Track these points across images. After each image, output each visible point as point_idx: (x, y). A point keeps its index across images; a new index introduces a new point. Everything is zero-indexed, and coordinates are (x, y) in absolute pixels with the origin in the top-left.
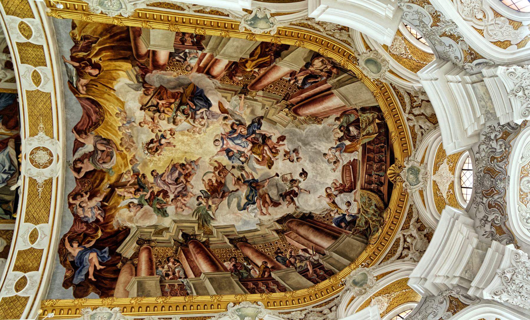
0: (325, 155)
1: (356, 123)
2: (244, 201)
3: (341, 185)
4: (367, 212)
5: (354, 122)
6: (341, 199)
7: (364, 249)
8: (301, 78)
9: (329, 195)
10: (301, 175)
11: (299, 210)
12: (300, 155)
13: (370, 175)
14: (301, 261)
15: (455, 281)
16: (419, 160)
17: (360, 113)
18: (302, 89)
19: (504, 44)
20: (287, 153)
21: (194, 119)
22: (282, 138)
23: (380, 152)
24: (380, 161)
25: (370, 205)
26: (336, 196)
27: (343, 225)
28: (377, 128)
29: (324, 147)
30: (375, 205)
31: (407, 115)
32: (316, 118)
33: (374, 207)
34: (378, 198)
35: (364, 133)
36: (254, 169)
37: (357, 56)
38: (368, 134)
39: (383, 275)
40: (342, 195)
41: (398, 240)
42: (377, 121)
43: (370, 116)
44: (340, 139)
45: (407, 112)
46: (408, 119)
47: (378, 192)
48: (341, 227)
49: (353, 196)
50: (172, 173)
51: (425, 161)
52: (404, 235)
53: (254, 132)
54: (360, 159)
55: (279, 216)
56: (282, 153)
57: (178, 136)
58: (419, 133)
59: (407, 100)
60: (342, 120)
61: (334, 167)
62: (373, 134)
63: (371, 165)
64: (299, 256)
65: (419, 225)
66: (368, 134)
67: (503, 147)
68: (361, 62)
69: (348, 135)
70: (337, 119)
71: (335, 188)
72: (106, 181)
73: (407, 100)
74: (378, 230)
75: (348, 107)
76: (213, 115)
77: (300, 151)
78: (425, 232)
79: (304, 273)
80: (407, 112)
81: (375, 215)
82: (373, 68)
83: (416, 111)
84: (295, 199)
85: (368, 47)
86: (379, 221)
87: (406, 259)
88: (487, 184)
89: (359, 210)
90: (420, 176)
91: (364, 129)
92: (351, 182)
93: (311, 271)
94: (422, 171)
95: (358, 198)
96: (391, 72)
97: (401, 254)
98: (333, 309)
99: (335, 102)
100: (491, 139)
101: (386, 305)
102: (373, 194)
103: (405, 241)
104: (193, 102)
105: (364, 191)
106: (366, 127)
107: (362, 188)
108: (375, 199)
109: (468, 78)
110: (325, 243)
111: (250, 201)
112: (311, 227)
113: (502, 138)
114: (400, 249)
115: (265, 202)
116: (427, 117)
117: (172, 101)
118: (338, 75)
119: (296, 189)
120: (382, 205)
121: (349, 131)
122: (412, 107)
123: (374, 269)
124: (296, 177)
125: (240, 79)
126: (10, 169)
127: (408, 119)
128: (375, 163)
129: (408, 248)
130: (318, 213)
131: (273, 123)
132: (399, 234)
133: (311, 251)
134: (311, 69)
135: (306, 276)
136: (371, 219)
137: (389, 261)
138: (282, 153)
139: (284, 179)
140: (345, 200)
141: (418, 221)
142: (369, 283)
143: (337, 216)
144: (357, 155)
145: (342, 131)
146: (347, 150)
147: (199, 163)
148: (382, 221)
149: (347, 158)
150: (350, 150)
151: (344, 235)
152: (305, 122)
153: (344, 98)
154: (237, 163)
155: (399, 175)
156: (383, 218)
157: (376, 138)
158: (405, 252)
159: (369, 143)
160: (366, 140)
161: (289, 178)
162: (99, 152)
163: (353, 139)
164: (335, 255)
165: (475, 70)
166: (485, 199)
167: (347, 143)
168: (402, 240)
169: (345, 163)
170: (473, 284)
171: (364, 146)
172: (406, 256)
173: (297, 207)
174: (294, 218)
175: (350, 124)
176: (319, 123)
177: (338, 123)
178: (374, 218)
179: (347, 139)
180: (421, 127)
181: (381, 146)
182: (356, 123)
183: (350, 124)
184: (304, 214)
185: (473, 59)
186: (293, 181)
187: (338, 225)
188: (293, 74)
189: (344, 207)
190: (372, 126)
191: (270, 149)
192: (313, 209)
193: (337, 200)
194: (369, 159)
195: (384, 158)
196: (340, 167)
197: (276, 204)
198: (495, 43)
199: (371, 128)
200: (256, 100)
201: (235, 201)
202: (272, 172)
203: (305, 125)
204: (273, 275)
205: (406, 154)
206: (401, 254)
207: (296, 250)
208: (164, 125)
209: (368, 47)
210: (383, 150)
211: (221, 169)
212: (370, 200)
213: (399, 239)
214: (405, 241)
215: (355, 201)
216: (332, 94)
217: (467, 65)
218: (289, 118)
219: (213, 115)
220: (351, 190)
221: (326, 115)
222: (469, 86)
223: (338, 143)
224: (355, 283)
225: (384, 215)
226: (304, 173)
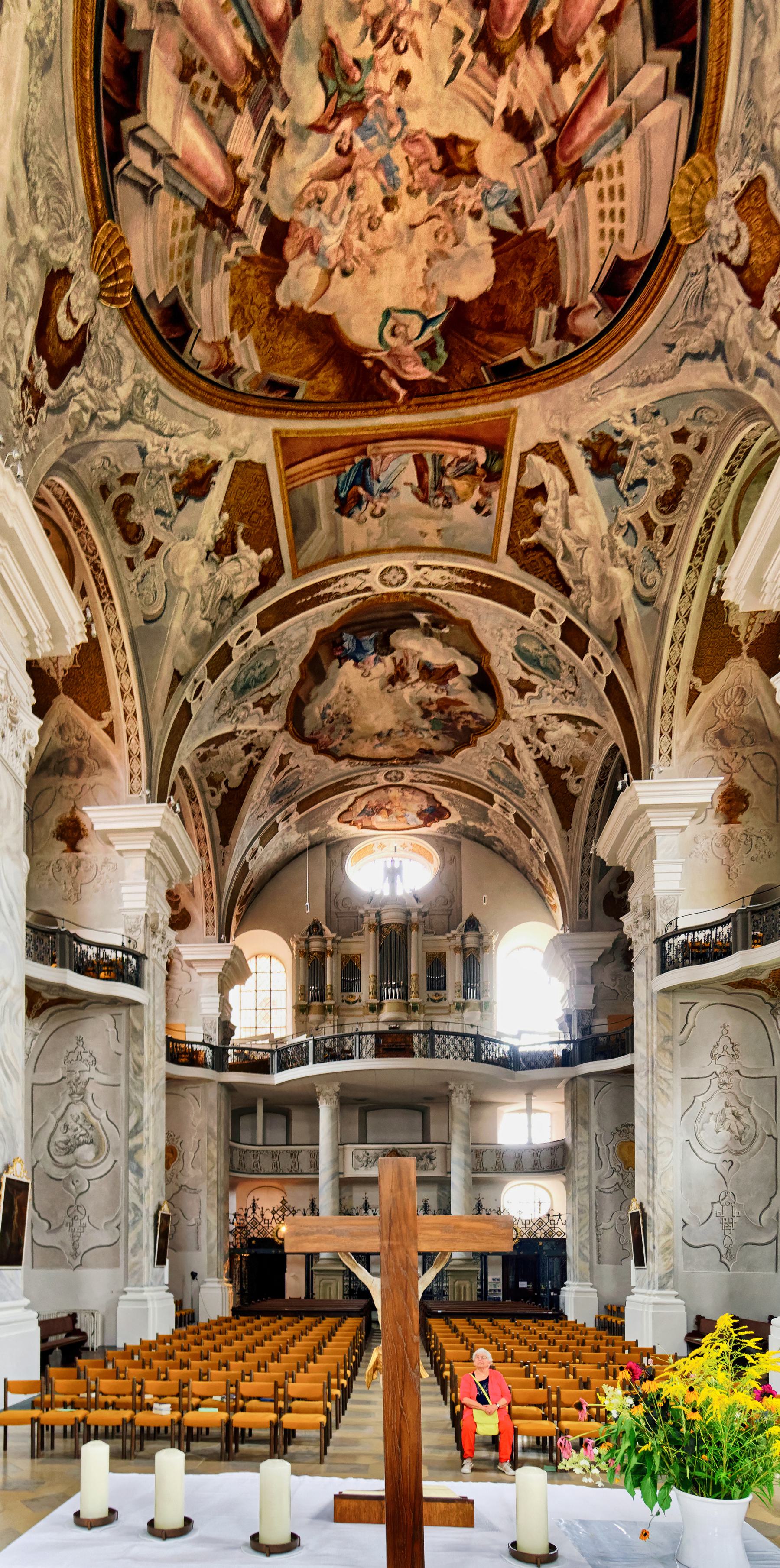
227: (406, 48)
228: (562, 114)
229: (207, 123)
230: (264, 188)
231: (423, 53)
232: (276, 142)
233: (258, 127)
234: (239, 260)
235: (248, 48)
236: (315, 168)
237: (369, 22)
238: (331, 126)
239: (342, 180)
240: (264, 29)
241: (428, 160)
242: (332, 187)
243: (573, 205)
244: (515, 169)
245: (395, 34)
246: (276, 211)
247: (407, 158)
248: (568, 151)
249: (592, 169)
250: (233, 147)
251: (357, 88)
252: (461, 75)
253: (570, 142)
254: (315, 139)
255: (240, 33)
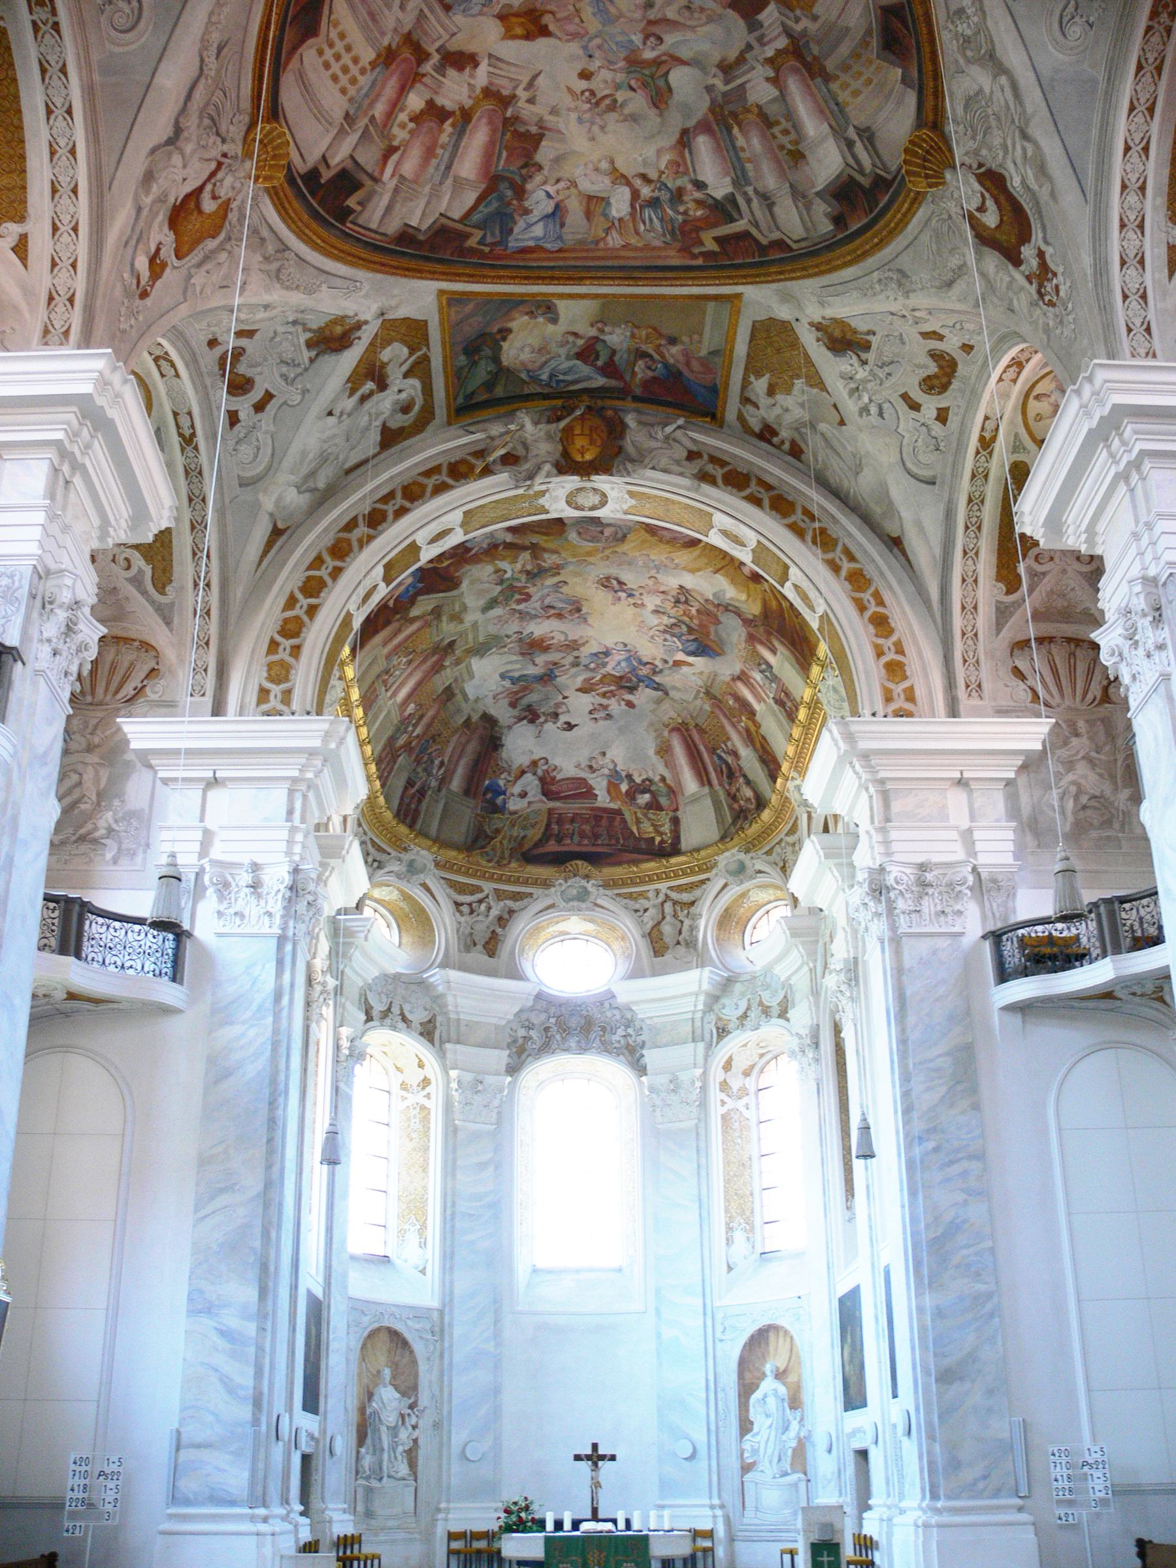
0: (604, 754)
1: (654, 805)
2: (516, 674)
3: (554, 778)
4: (514, 825)
5: (657, 802)
6: (530, 782)
7: (457, 848)
8: (730, 759)
9: (534, 763)
10: (568, 723)
11: (505, 731)
12: (601, 722)
13: (572, 821)
14: (425, 770)
15: (453, 1016)
16: (599, 901)
17: (671, 814)
18: (713, 751)
19: (728, 1066)
20: (605, 707)
21: (665, 632)
22: (630, 705)
23: (610, 837)
24: (596, 836)
25: (524, 828)
26: (535, 774)
27: (489, 796)
28: (647, 836)
29: (619, 755)
30: (525, 837)
31: (664, 891)
32: (664, 751)
33: (522, 834)
34: (539, 836)
35: (639, 815)
36: (575, 676)
37: (751, 854)
38: (638, 822)
39: (428, 889)
40: (537, 782)
41: (479, 889)
42: (658, 839)
43: (667, 828)
44: (629, 777)
45: (669, 892)
46: (658, 892)
47: (547, 835)
48: (484, 795)
49: (537, 799)
50: (560, 600)
51: (597, 909)
52: (487, 897)
53: (640, 681)
54: (597, 805)
55: (493, 712)
56: (605, 702)
57: (631, 611)
58: (637, 906)
59: (686, 897)
60: (661, 785)
61: (583, 766)
62: (638, 829)
63: (587, 821)
64: (432, 762)
65: (506, 916)
66: (638, 822)
67: (616, 1045)
68: (742, 856)
69: (636, 790)
70: (663, 779)
71: (547, 771)
72: (545, 538)
73: (686, 897)
74: (489, 861)
75: (680, 799)
76: (671, 651)
77: (608, 722)
78: (499, 930)
79: (410, 783)
80: (669, 892)
81: (510, 841)
82: (734, 867)
83: (668, 907)
84: (525, 722)
85: (760, 872)
86: (502, 858)
87: (457, 914)
88: (573, 1022)
89: (515, 813)
90: (575, 903)
91: (645, 815)
92: (557, 793)
93: (413, 791)
94: (583, 905)
95: (534, 807)
96: (725, 885)
97: (462, 904)
98: (376, 864)
99: (690, 784)
100: (627, 1027)
101: (387, 898)
102: (542, 830)
103: (480, 901)
104: (693, 640)
105: (546, 815)
106: (649, 819)
107: (550, 812)
108: (535, 834)
109: (699, 1015)
110: (456, 784)
111: (514, 681)
112: (479, 756)
113: (628, 1044)
114: (468, 899)
115: (516, 693)
116: (659, 923)
117: (696, 621)
118: (731, 808)
119: (542, 719)
120: (527, 847)
121: (643, 792)
122: (675, 903)
123: (434, 875)
124: (563, 718)
125: (731, 702)
126: (558, 382)
127: (658, 892)
128: (593, 827)
129: (472, 912)
130: (504, 755)
131: (658, 702)
132: (488, 887)
133: (442, 771)
134: (741, 780)
135: (406, 789)
136: (504, 838)
137: (449, 890)
138: (605, 702)
139: (558, 705)
140: (528, 789)
141: (511, 912)
142: (415, 878)
143: (501, 783)
144: (603, 799)
145: (643, 781)
146: (612, 787)
147: (583, 626)
148: (505, 862)
149: (600, 786)
150: (612, 790)
151: (472, 802)
152: (659, 736)
153: (695, 799)
154: (584, 661)
155: (575, 876)
156: (509, 862)
157: (632, 833)
158: (465, 909)
159: (624, 821)
160: (628, 816)
161: (560, 711)
162: (599, 529)
163: (631, 795)
164: (441, 806)
165: (707, 1026)
166: (553, 1020)
167: (624, 787)
168: (480, 896)
169: (591, 782)
170: (458, 1046)
171: (618, 812)
172: (461, 913)
173: (510, 727)
174: (492, 728)
175: (654, 795)
176: (658, 753)
177: (657, 778)
178: (505, 842)
179: (631, 788)
180: (646, 910)
181: (618, 840)
182: (654, 805)
183: (654, 795)
184: (500, 739)
185: (718, 1028)
186: (556, 715)
187: (488, 789)
188: (735, 754)
189: (517, 789)
190: (651, 829)
191: (611, 692)
192: (510, 747)
193: (529, 777)
194: (598, 818)
195: (600, 842)
196: (582, 775)
197: (513, 705)
198: (731, 1057)
199: (648, 829)
200: (696, 698)
201: (519, 666)
202: (571, 692)
203: (654, 734)
204: (401, 758)
205: (606, 885)
206: (462, 904)
207: (441, 752)
208: (652, 602)
209: (760, 872)
210: (613, 842)
211: (573, 646)
212: (533, 826)
213: (482, 891)
214: (480, 901)
215: (529, 803)
216: (702, 784)
217: (712, 1017)
218: (666, 719)
219: (671, 651)
220: (547, 793)
221: (670, 764)
222: (690, 1016)
223: (624, 774)
224: (411, 864)
225: (514, 865)
226: (570, 727)
227: (583, 93)
228: (418, 85)
229: (790, 115)
230: (749, 47)
231: (565, 90)
232: (727, 69)
233: (742, 86)
234: (798, 12)
235: (736, 130)
236: (689, 35)
237: (618, 110)
238: (664, 58)
239: (659, 16)
240: (719, 135)
241: (558, 20)
242: (671, 14)
243: (383, 34)
244: (455, 30)
245: (593, 101)
246: (741, 23)
247: (582, 21)
248: (403, 66)
249: (373, 69)
250: (772, 92)
251: (633, 75)
252: (526, 80)
253: (402, 73)
254: (684, 53)
255: (740, 141)
